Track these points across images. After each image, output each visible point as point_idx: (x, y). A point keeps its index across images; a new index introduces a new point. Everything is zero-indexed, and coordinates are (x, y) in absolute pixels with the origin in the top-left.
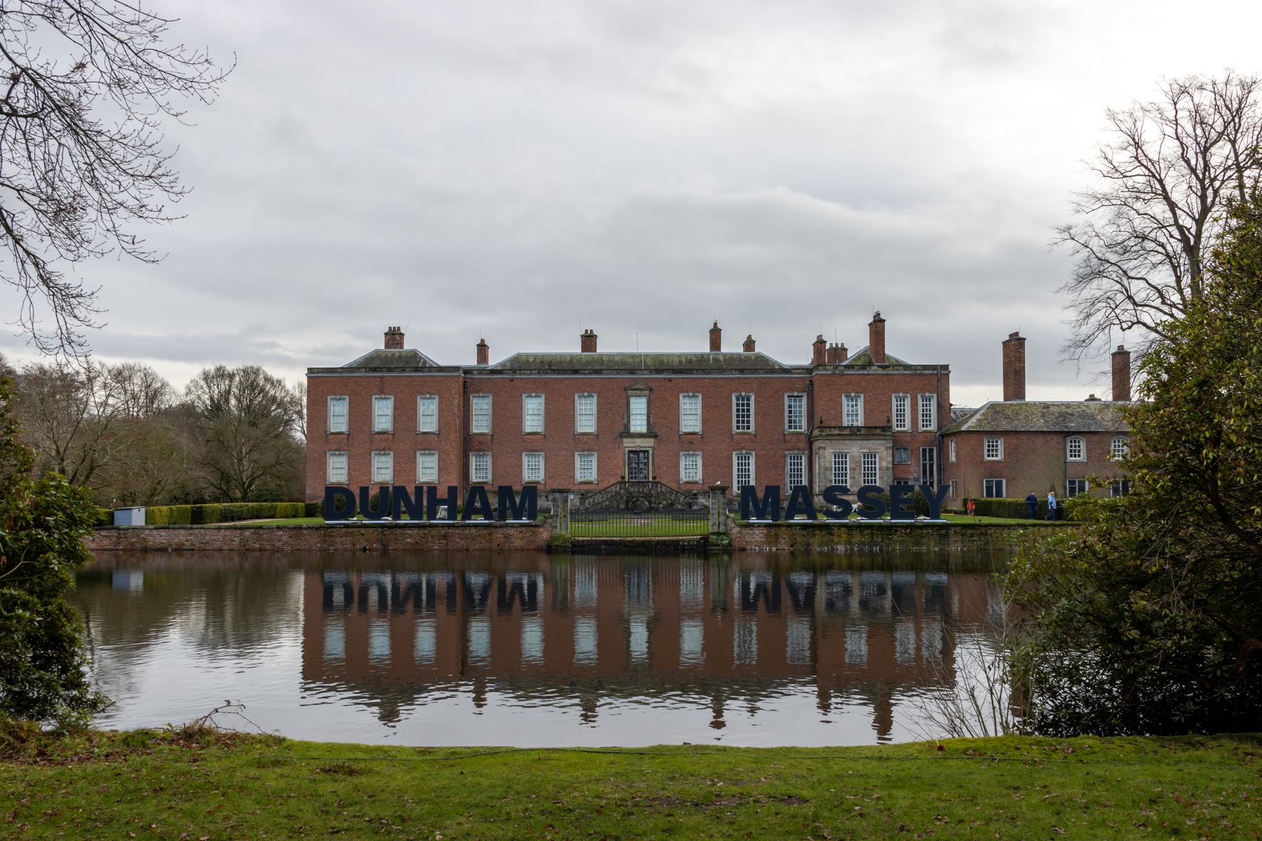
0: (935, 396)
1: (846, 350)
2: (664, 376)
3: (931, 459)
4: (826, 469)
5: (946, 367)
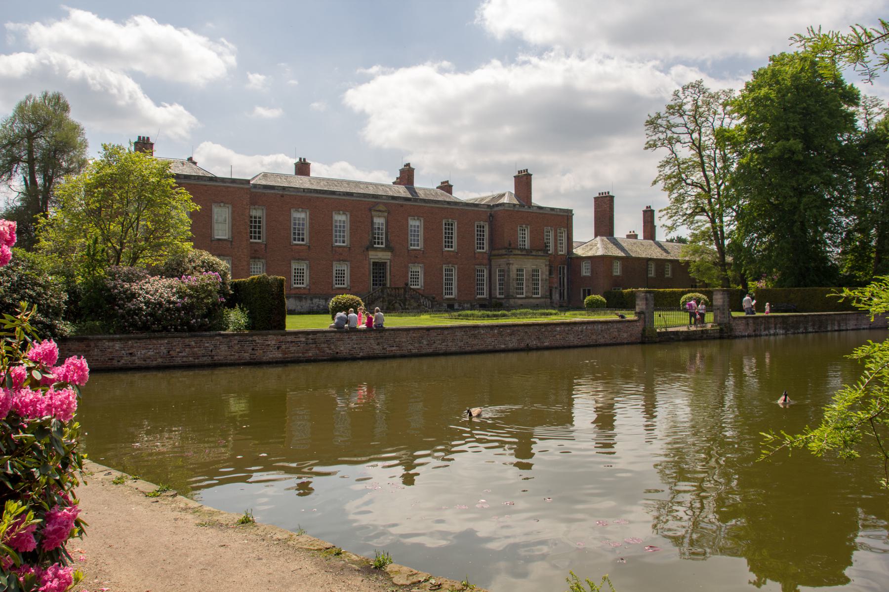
5: (571, 211)
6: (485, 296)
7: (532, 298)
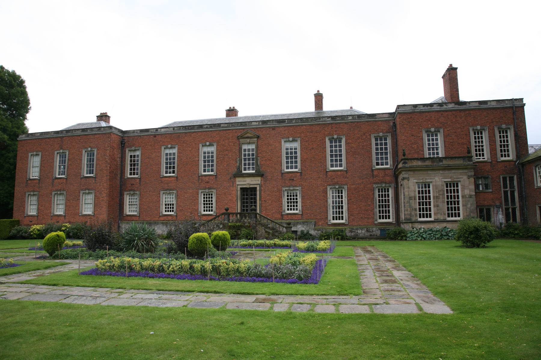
0: (512, 127)
3: (512, 186)
4: (410, 198)
6: (390, 220)
7: (445, 221)
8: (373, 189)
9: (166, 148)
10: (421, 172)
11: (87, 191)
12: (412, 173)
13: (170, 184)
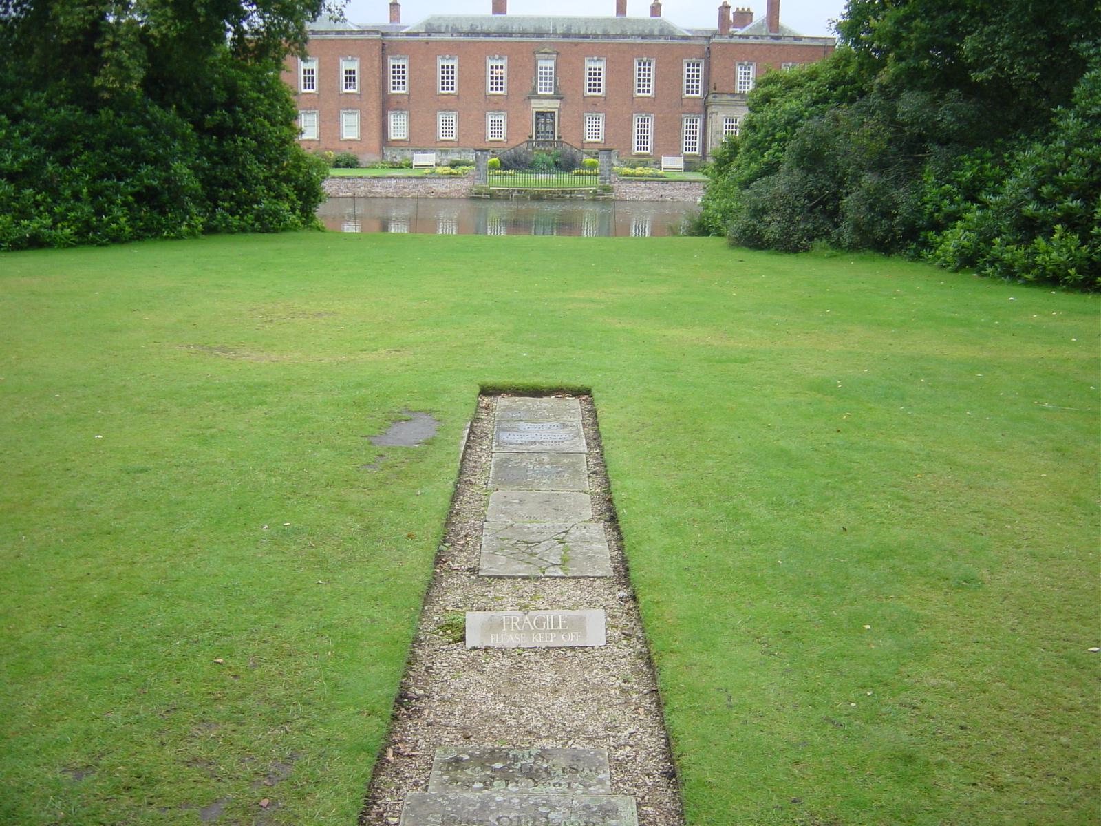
1: (752, 14)
2: (571, 42)
4: (717, 133)
8: (682, 120)
9: (443, 58)
10: (728, 107)
11: (350, 111)
12: (721, 107)
13: (449, 104)
